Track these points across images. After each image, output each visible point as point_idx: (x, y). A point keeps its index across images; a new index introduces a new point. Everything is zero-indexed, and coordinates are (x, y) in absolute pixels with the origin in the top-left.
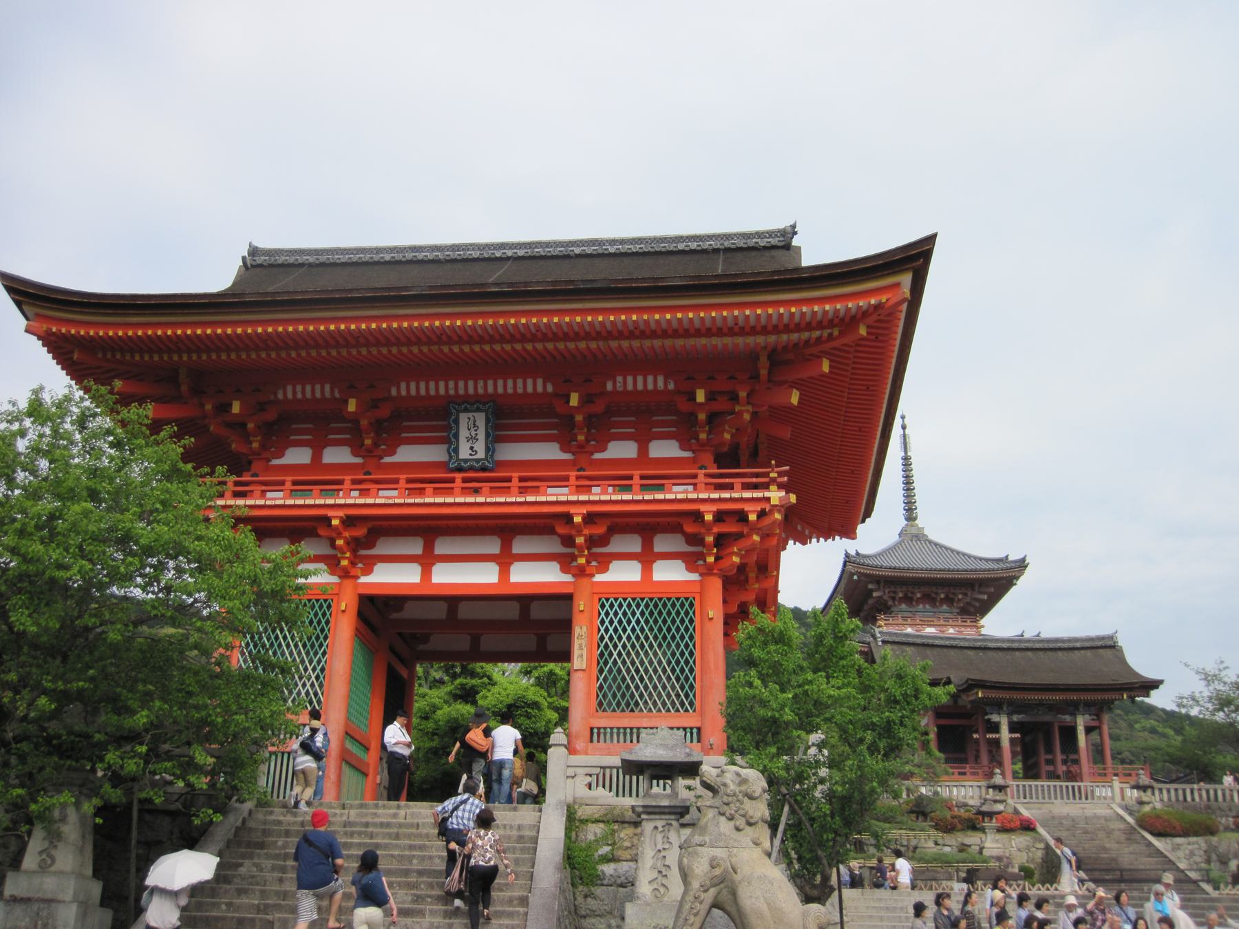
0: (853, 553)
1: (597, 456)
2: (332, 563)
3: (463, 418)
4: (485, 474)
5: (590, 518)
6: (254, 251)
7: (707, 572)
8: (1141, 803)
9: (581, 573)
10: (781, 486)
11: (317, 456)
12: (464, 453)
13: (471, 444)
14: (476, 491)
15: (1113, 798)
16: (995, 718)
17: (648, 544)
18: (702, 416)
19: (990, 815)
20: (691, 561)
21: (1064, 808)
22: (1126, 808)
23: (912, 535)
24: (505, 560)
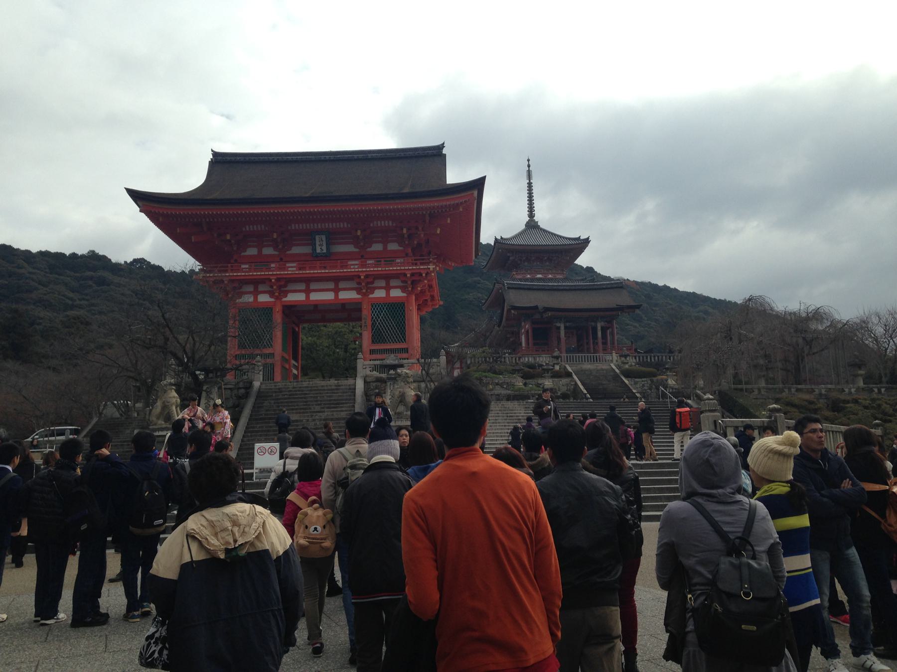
0: (499, 238)
1: (369, 249)
2: (271, 294)
3: (317, 237)
4: (328, 258)
5: (367, 276)
6: (215, 154)
7: (409, 293)
8: (624, 363)
9: (365, 295)
10: (434, 264)
11: (260, 251)
12: (318, 250)
13: (321, 247)
14: (325, 268)
15: (612, 361)
16: (558, 325)
17: (388, 284)
18: (406, 236)
19: (548, 370)
20: (403, 289)
21: (587, 366)
22: (618, 367)
23: (532, 225)
24: (336, 290)
